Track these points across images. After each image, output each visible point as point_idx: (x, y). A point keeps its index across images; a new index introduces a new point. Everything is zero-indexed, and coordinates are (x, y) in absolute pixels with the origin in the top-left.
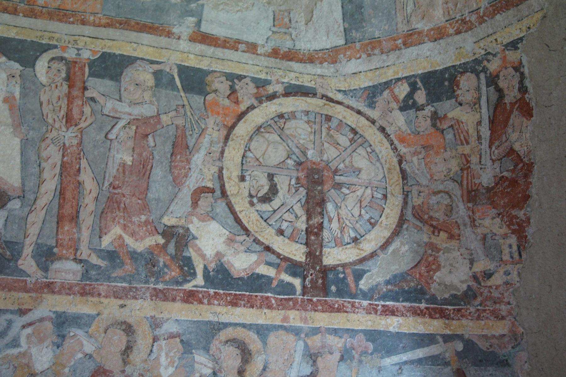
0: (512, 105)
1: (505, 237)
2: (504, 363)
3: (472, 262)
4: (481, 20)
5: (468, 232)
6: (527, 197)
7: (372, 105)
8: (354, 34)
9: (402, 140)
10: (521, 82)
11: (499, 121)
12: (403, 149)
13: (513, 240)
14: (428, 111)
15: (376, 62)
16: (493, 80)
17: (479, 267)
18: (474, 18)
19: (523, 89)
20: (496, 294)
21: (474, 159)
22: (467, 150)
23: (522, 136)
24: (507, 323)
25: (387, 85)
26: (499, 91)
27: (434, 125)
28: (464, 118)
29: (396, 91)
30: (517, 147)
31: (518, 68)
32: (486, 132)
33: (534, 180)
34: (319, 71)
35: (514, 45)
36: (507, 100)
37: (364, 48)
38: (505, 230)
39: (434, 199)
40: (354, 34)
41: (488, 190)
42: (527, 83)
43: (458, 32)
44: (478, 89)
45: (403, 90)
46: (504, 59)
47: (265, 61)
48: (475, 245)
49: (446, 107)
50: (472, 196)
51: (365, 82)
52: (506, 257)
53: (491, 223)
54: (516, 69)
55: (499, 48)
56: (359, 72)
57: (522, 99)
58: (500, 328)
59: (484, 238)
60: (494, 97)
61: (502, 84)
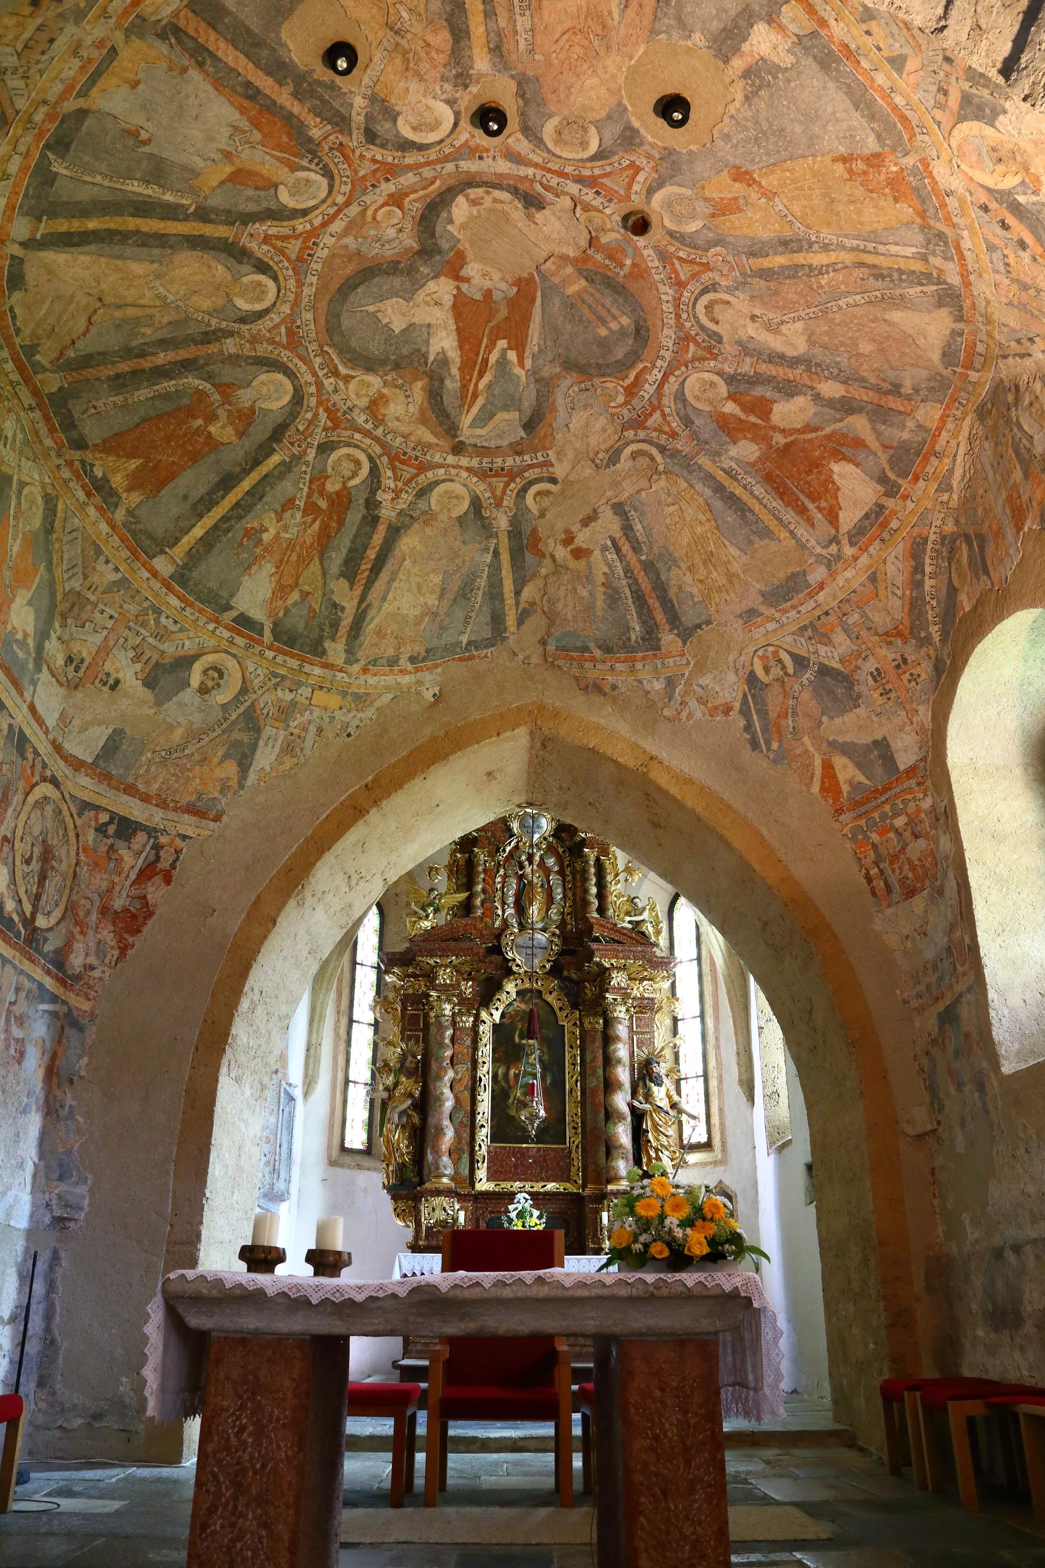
0: (161, 870)
1: (112, 948)
2: (81, 1030)
3: (87, 955)
4: (175, 810)
5: (91, 933)
6: (139, 931)
7: (80, 815)
8: (102, 764)
9: (85, 851)
10: (175, 861)
11: (146, 873)
12: (82, 857)
13: (116, 953)
14: (110, 841)
15: (103, 788)
16: (157, 848)
17: (89, 961)
18: (172, 805)
19: (173, 866)
20: (91, 983)
21: (117, 888)
22: (117, 879)
23: (156, 892)
24: (91, 1004)
25: (97, 808)
26: (158, 858)
27: (108, 852)
28: (126, 859)
29: (100, 816)
30: (149, 897)
31: (178, 852)
32: (133, 876)
33: (150, 923)
34: (66, 771)
35: (184, 837)
36: (159, 866)
37: (99, 775)
38: (113, 943)
39: (83, 902)
40: (102, 764)
41: (116, 912)
42: (178, 864)
43: (157, 805)
44: (144, 846)
45: (104, 818)
46: (172, 841)
47: (46, 743)
48: (92, 945)
49: (121, 844)
50: (104, 910)
51: (86, 797)
52: (107, 961)
53: (107, 935)
54: (176, 852)
55: (174, 832)
56: (84, 786)
57: (169, 872)
58: (86, 1006)
59: (99, 942)
60: (152, 858)
61: (162, 853)
